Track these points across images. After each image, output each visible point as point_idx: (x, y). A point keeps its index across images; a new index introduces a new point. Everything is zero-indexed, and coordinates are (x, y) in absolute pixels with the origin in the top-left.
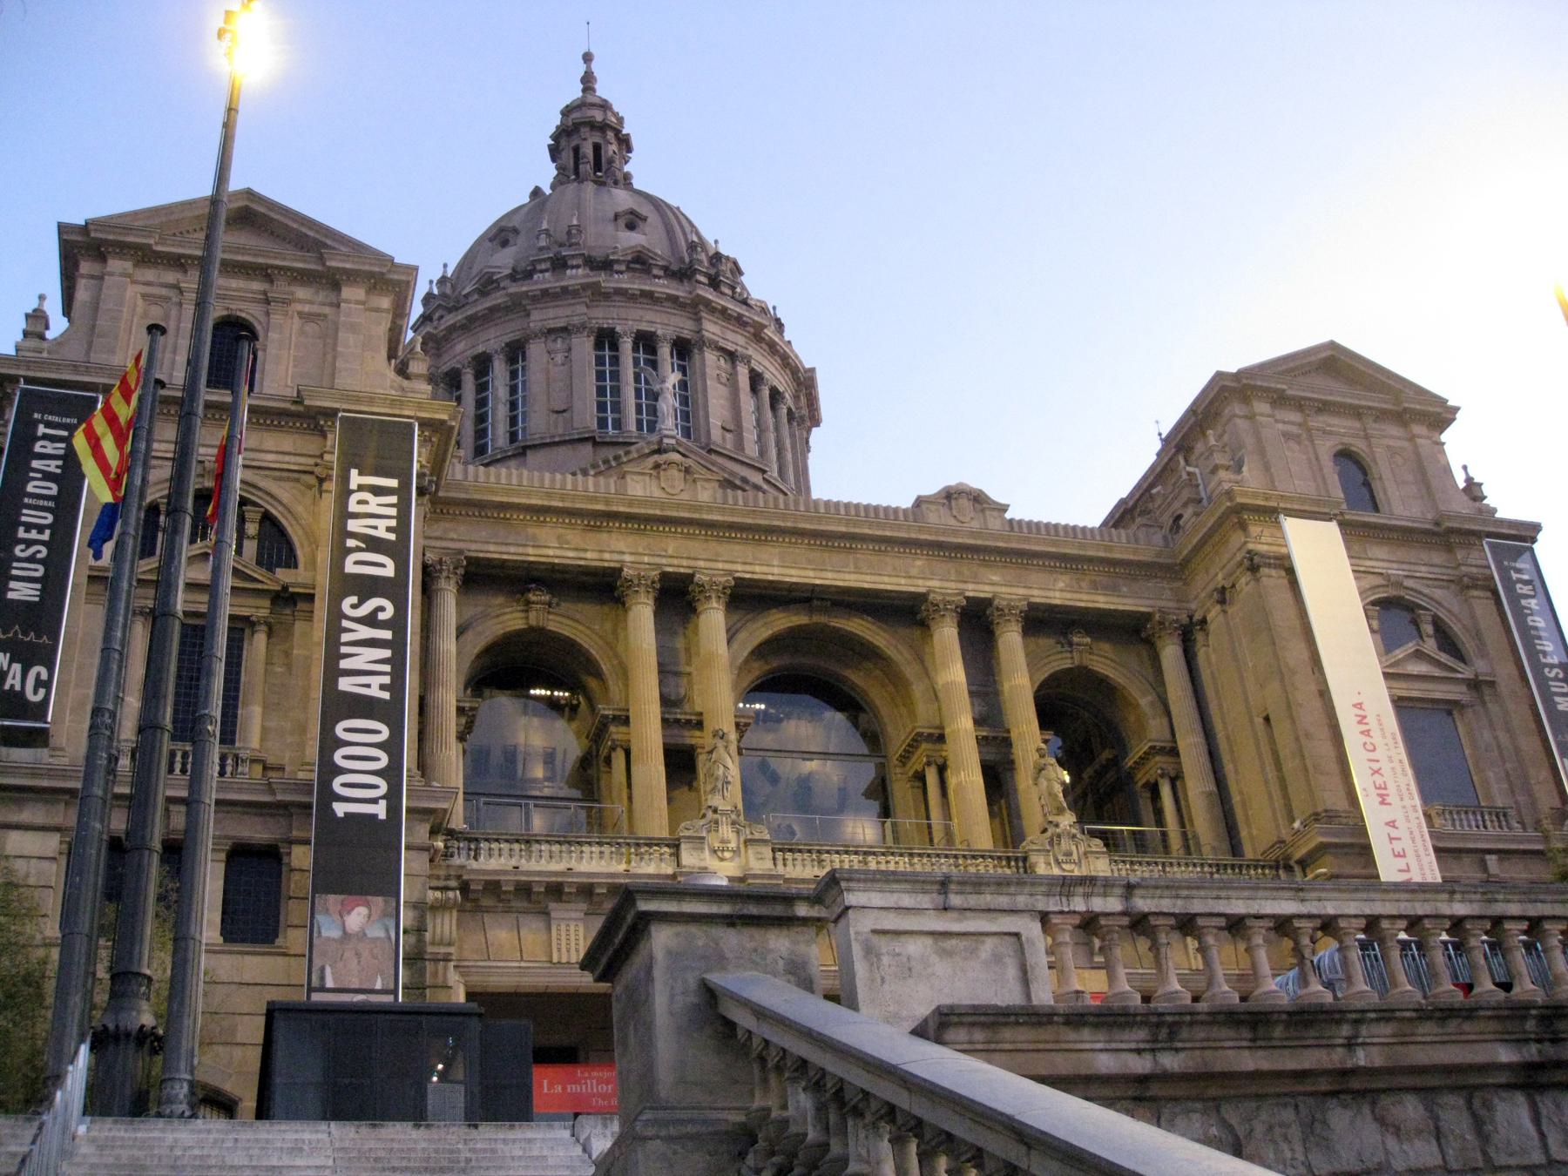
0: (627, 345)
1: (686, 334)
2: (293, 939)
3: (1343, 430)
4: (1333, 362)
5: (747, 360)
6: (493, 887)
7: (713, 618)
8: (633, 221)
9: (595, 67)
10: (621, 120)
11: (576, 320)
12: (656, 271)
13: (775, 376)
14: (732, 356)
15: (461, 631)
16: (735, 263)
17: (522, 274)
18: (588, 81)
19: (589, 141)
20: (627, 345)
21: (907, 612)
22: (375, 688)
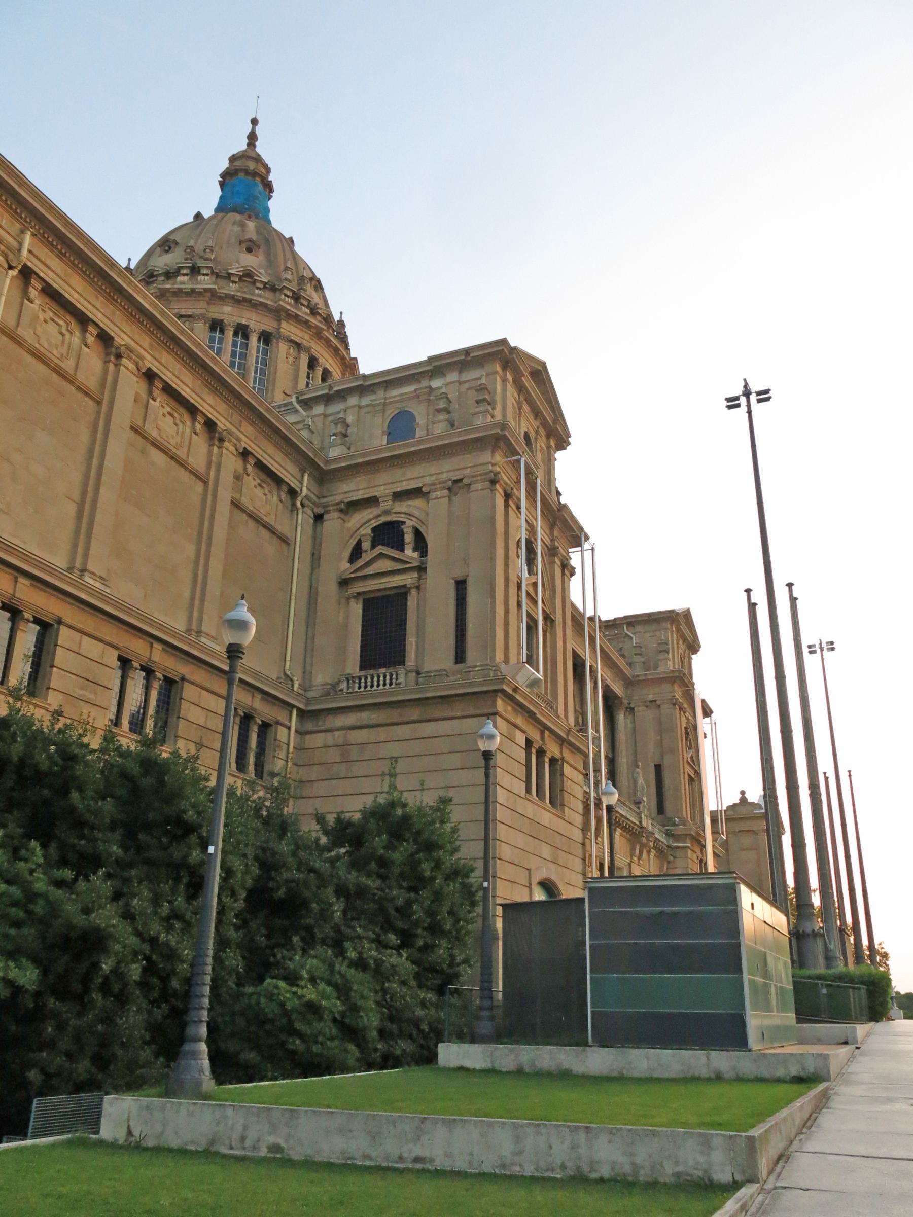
0: (230, 333)
1: (269, 329)
5: (308, 350)
9: (259, 130)
10: (268, 170)
11: (198, 312)
12: (258, 285)
13: (327, 361)
14: (298, 346)
16: (319, 281)
18: (252, 138)
19: (246, 180)
20: (230, 333)
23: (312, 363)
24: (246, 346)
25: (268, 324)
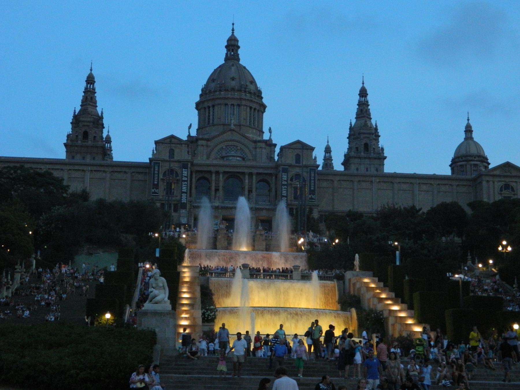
2: (178, 212)
3: (298, 151)
4: (298, 142)
6: (196, 206)
7: (221, 176)
8: (233, 79)
15: (195, 177)
17: (215, 91)
20: (230, 106)
21: (243, 173)
22: (185, 191)
23: (251, 108)
24: (234, 109)
25: (239, 102)
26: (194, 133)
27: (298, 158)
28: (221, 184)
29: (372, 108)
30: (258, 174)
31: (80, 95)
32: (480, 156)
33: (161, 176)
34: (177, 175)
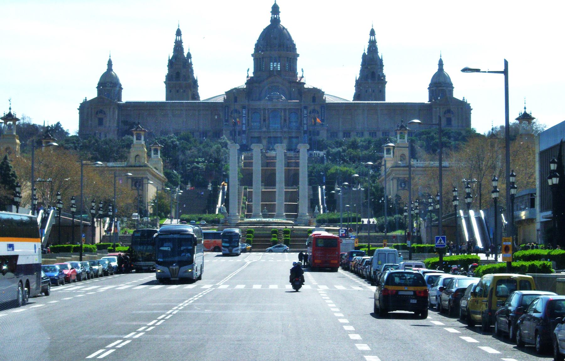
26: (251, 75)
27: (314, 99)
28: (267, 116)
29: (378, 45)
30: (289, 109)
31: (173, 45)
32: (446, 83)
33: (230, 114)
34: (239, 113)
